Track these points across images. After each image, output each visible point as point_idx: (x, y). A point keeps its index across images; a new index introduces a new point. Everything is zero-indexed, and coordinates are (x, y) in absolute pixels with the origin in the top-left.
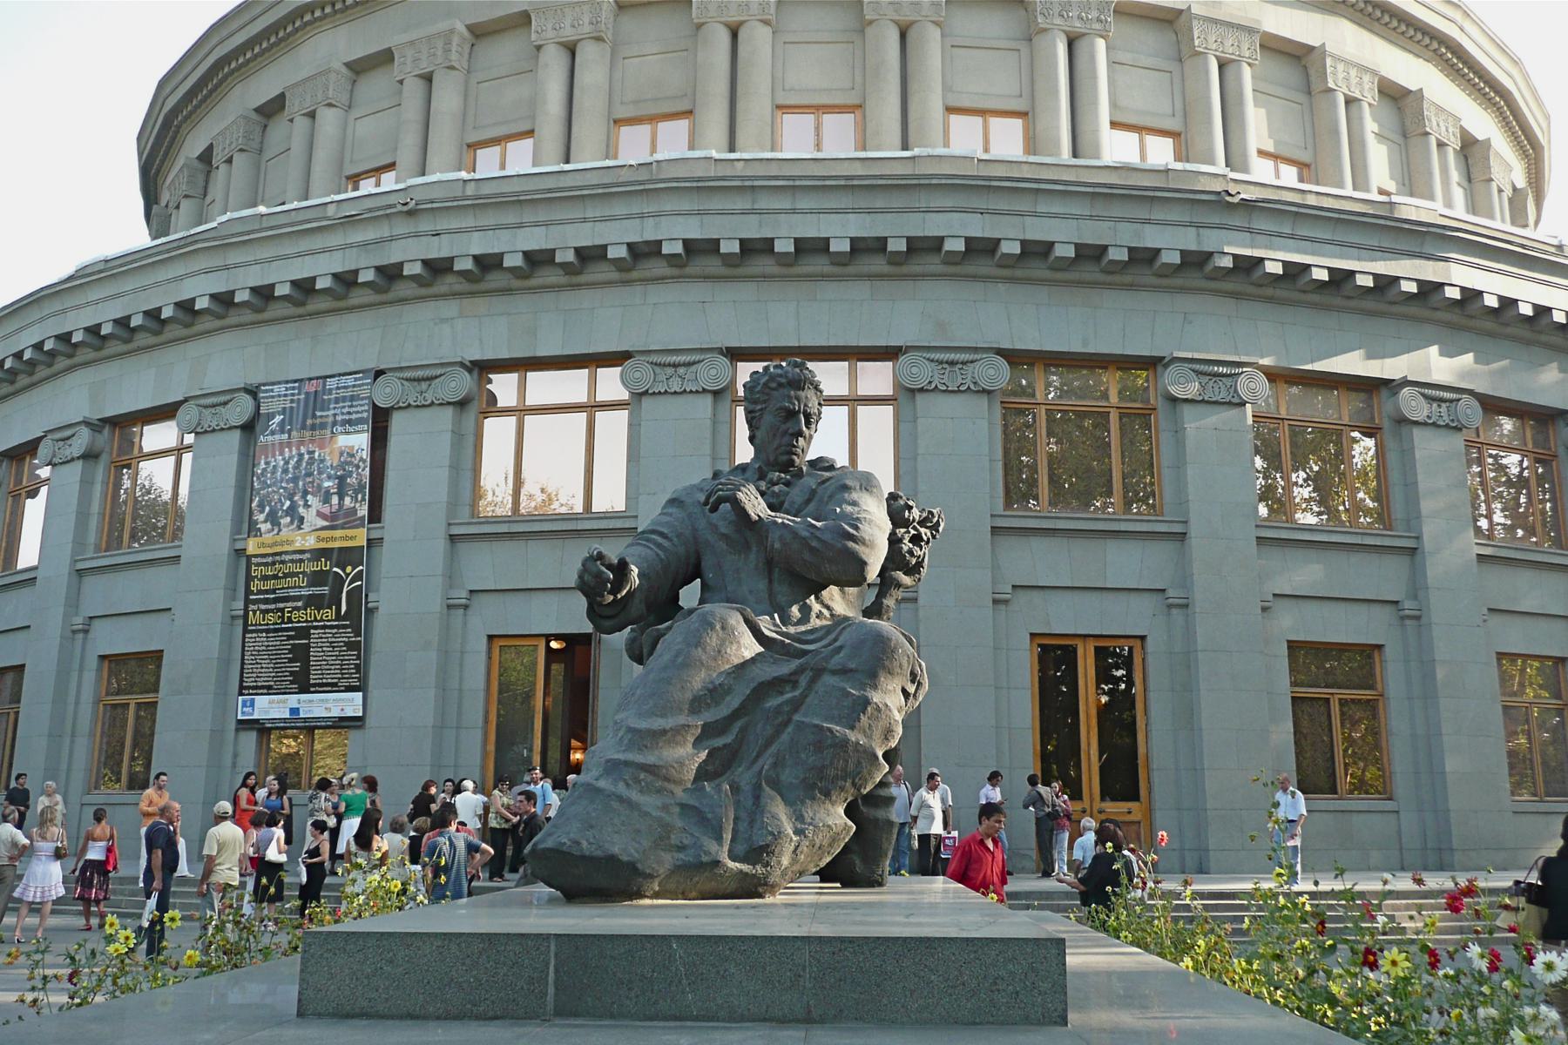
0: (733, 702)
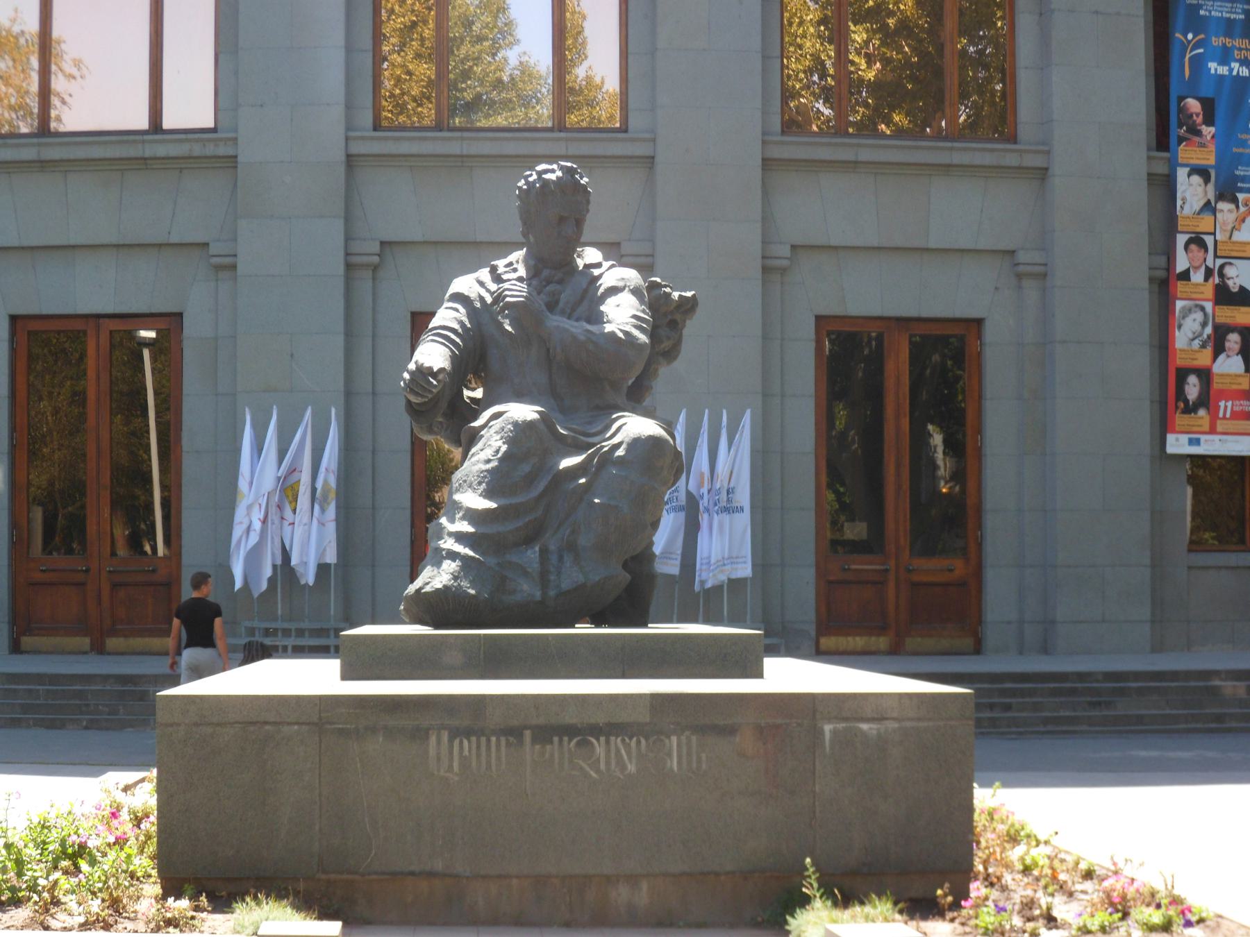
0: (541, 486)
